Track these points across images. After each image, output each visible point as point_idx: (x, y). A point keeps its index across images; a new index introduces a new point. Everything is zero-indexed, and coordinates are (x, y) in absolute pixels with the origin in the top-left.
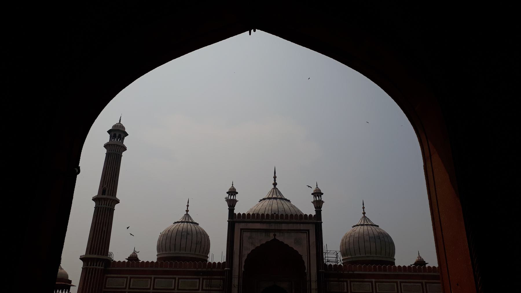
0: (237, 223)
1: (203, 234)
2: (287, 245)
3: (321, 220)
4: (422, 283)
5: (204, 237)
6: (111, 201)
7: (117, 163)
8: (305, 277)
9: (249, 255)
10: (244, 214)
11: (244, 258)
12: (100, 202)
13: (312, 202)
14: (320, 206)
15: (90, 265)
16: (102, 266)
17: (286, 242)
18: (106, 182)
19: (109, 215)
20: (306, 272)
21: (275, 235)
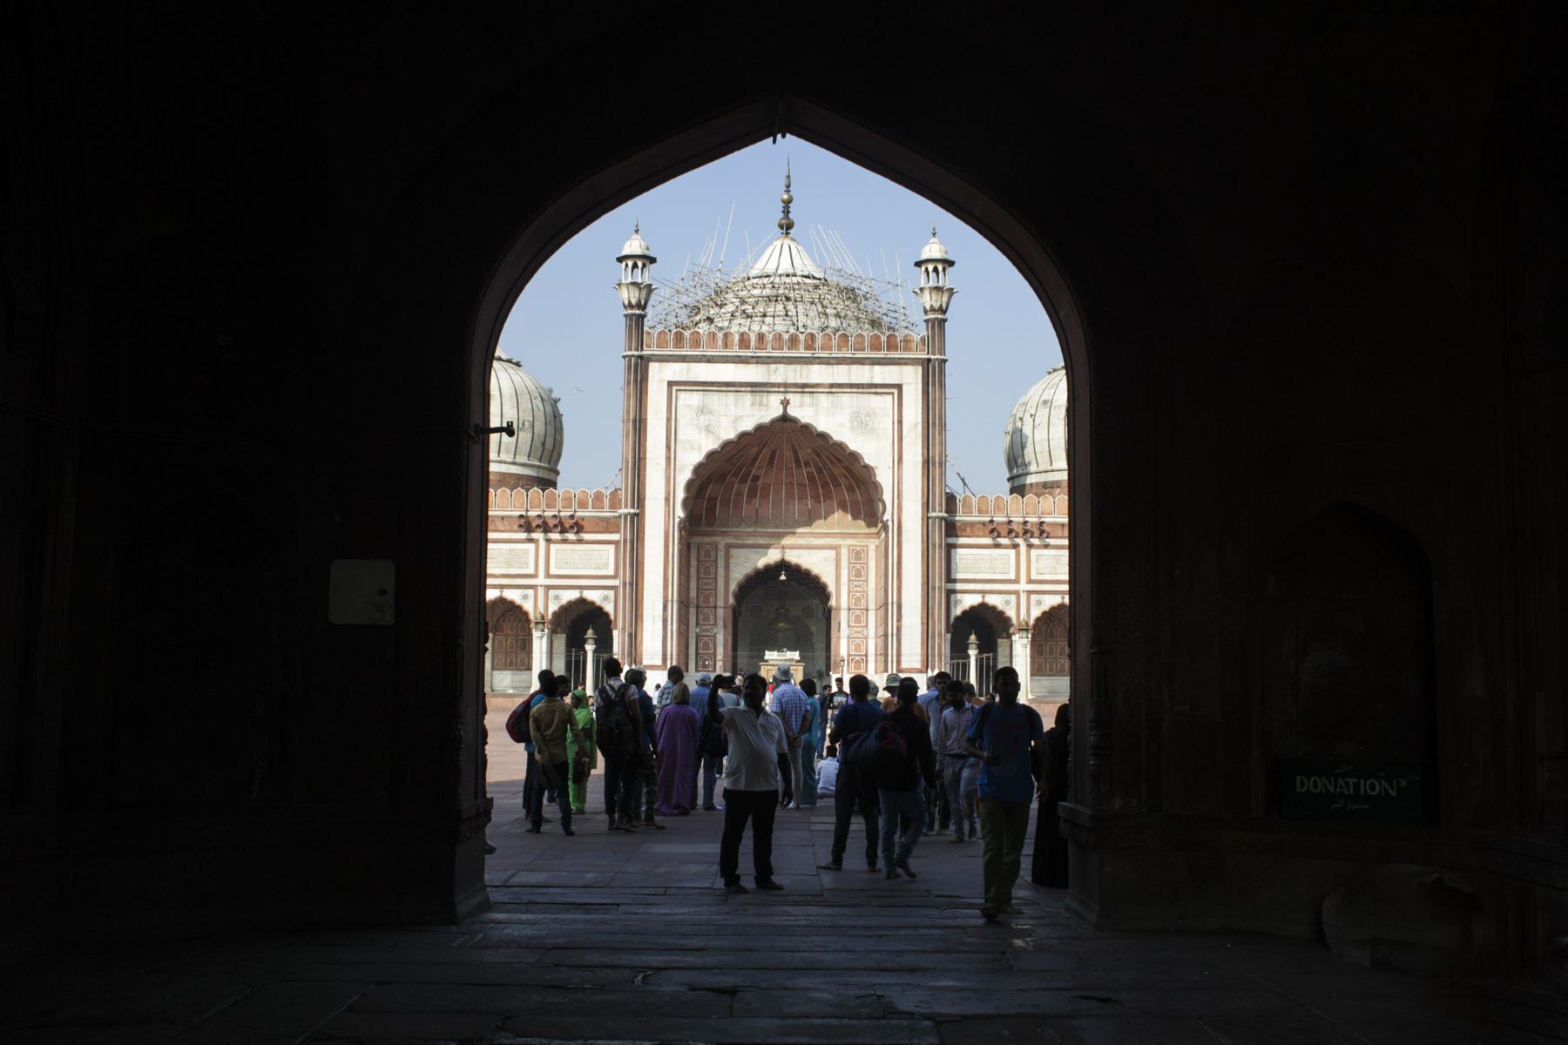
0: (657, 364)
1: (540, 399)
2: (824, 436)
3: (942, 351)
5: (542, 408)
8: (883, 535)
9: (698, 469)
11: (684, 475)
14: (941, 305)
17: (821, 425)
21: (785, 403)
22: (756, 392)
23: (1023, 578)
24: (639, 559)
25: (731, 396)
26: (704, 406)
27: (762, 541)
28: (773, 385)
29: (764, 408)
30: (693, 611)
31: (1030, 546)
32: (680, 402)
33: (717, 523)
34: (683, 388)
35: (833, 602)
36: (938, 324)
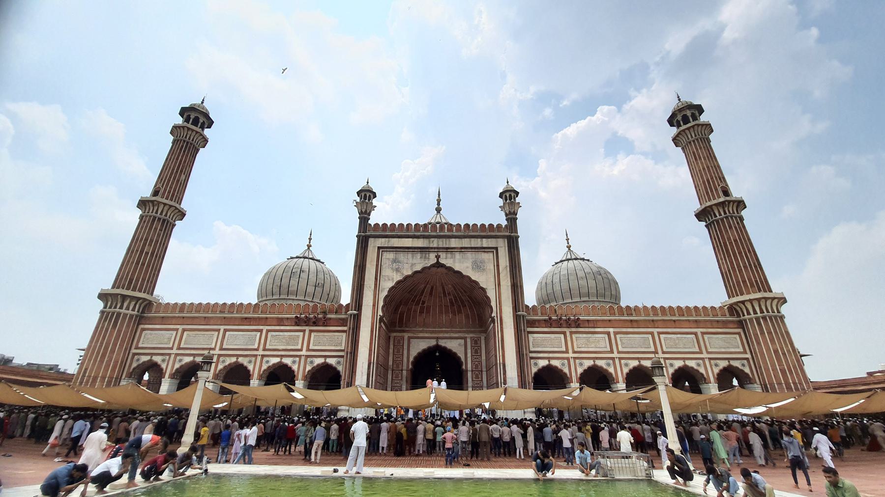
2: (459, 273)
4: (695, 334)
5: (329, 279)
6: (166, 208)
7: (187, 156)
8: (492, 324)
10: (385, 225)
11: (385, 293)
12: (145, 209)
13: (500, 207)
15: (110, 308)
16: (133, 310)
18: (162, 180)
19: (161, 230)
20: (493, 316)
21: (438, 257)
22: (423, 251)
23: (570, 351)
24: (357, 339)
25: (410, 255)
26: (396, 259)
27: (427, 335)
28: (432, 248)
29: (427, 259)
30: (390, 372)
31: (571, 333)
32: (384, 257)
33: (404, 325)
34: (386, 250)
35: (464, 367)
36: (512, 218)
